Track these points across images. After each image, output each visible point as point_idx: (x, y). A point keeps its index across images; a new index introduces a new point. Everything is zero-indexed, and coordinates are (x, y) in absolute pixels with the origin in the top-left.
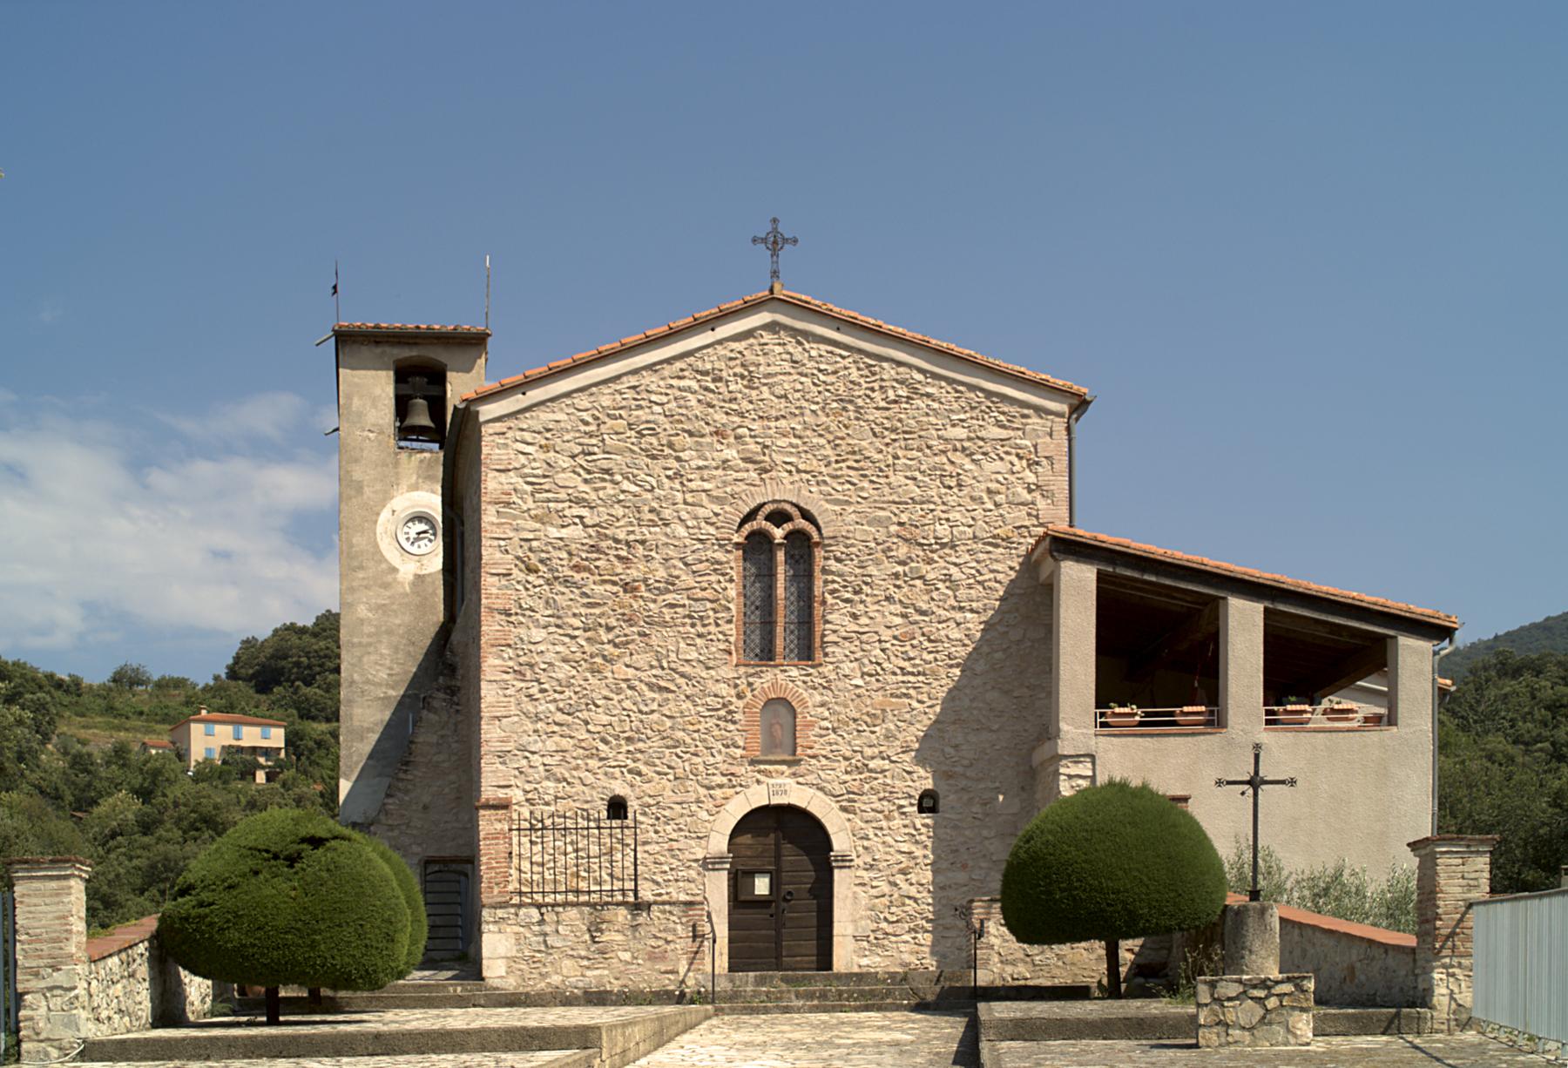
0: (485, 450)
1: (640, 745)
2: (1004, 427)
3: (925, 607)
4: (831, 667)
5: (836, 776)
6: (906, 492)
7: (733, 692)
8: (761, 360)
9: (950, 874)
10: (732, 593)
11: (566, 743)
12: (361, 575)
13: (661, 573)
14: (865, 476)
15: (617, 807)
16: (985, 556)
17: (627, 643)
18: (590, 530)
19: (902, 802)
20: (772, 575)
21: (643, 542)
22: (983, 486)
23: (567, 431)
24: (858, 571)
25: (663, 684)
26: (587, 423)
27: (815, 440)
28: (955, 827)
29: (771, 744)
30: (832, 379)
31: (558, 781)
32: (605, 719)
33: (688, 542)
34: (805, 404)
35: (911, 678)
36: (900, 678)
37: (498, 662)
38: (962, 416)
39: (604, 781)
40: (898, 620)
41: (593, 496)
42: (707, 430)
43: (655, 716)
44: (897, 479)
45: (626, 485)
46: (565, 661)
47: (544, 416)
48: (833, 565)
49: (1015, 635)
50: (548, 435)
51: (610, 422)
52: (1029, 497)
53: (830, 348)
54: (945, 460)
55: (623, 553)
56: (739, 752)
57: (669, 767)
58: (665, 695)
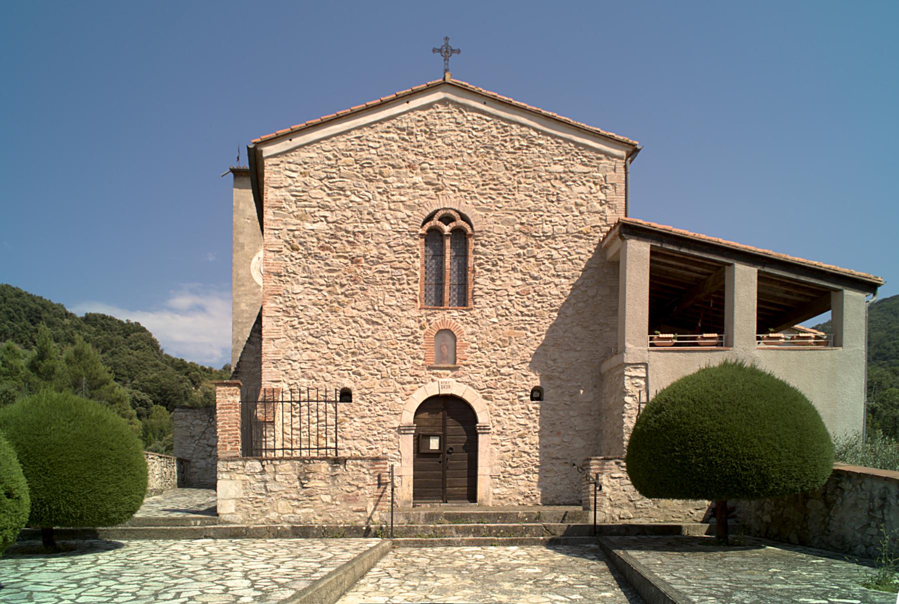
0: (266, 175)
1: (360, 357)
2: (586, 165)
3: (536, 275)
4: (478, 311)
5: (480, 377)
6: (526, 204)
7: (418, 325)
8: (437, 122)
9: (550, 438)
10: (418, 264)
11: (314, 355)
13: (375, 252)
14: (500, 194)
15: (346, 395)
16: (573, 244)
17: (353, 294)
18: (331, 225)
19: (521, 394)
20: (442, 255)
21: (363, 233)
22: (573, 201)
23: (318, 164)
24: (495, 252)
25: (375, 319)
26: (329, 159)
27: (470, 172)
28: (553, 410)
29: (441, 357)
30: (480, 134)
31: (310, 378)
32: (339, 341)
33: (391, 233)
34: (464, 149)
35: (527, 318)
36: (520, 318)
37: (273, 305)
38: (560, 158)
39: (338, 379)
40: (520, 283)
41: (333, 204)
42: (404, 164)
43: (370, 339)
44: (520, 196)
45: (353, 198)
46: (314, 305)
47: (303, 154)
48: (480, 248)
49: (591, 292)
50: (306, 166)
51: (344, 159)
52: (601, 209)
53: (480, 115)
54: (549, 185)
55: (351, 239)
56: (421, 362)
57: (378, 371)
58: (376, 327)
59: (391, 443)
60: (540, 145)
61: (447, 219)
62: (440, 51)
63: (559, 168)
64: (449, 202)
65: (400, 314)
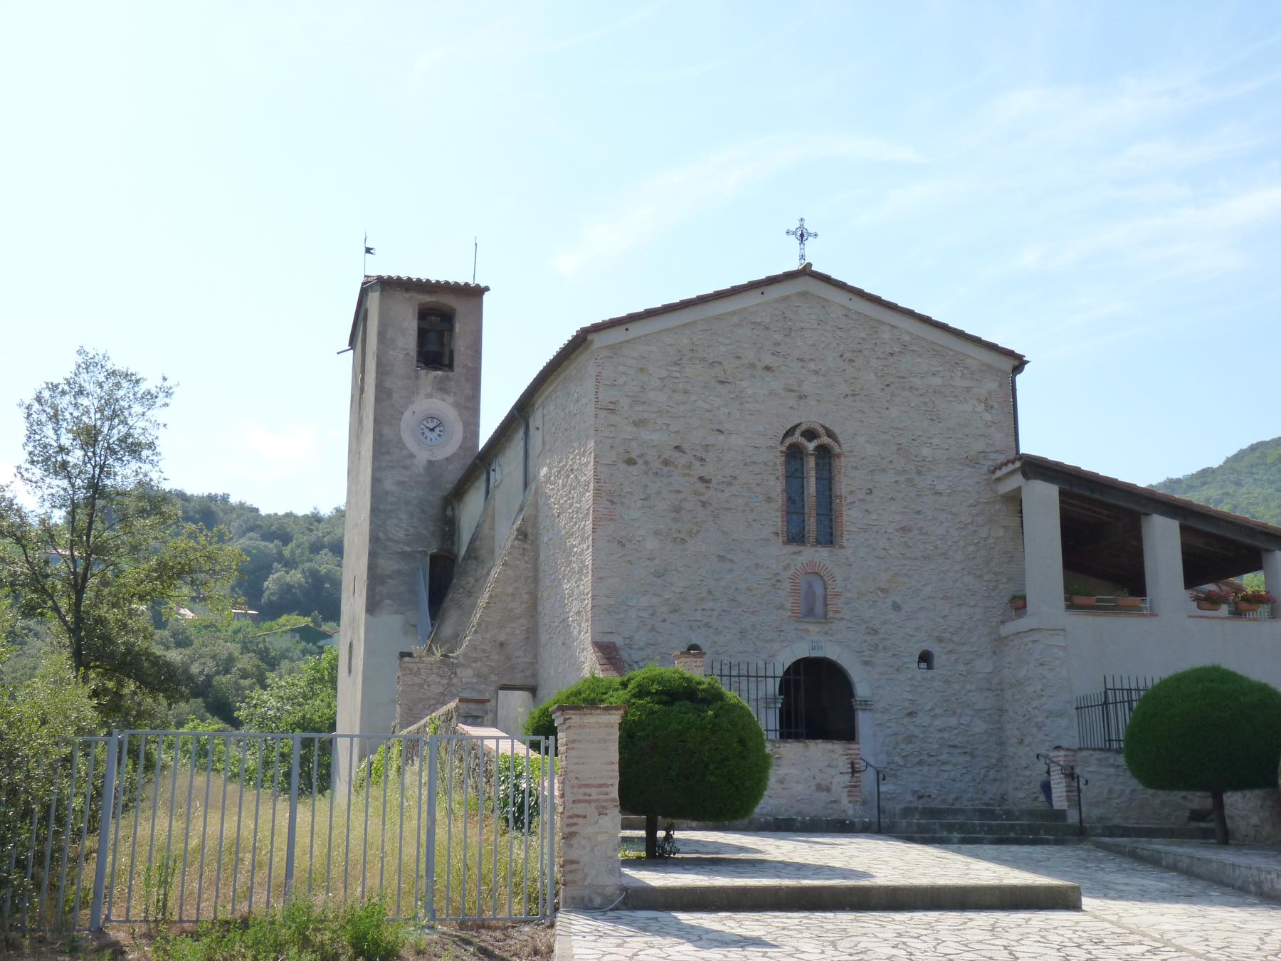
12: (388, 458)
28: (947, 682)
55: (698, 454)
60: (913, 351)
61: (810, 434)
62: (794, 233)
63: (937, 381)
64: (810, 416)
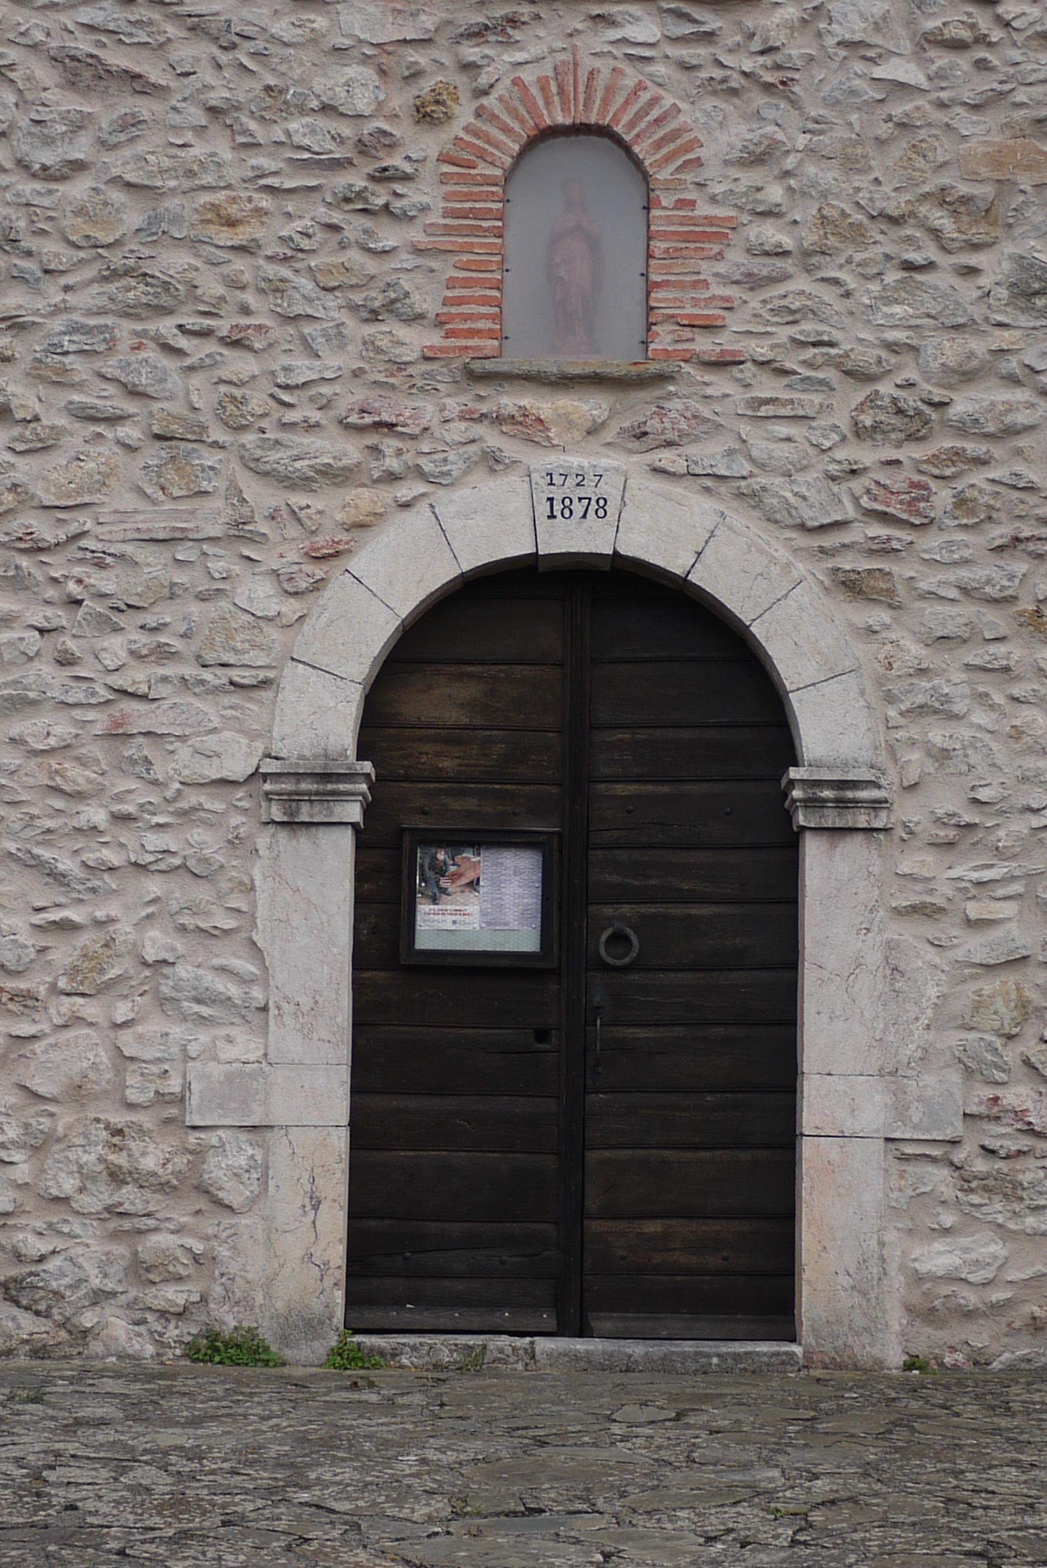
7: (401, 100)
25: (116, 59)
43: (79, 189)
56: (414, 340)
57: (135, 393)
58: (129, 104)
59: (202, 893)
65: (281, 28)
